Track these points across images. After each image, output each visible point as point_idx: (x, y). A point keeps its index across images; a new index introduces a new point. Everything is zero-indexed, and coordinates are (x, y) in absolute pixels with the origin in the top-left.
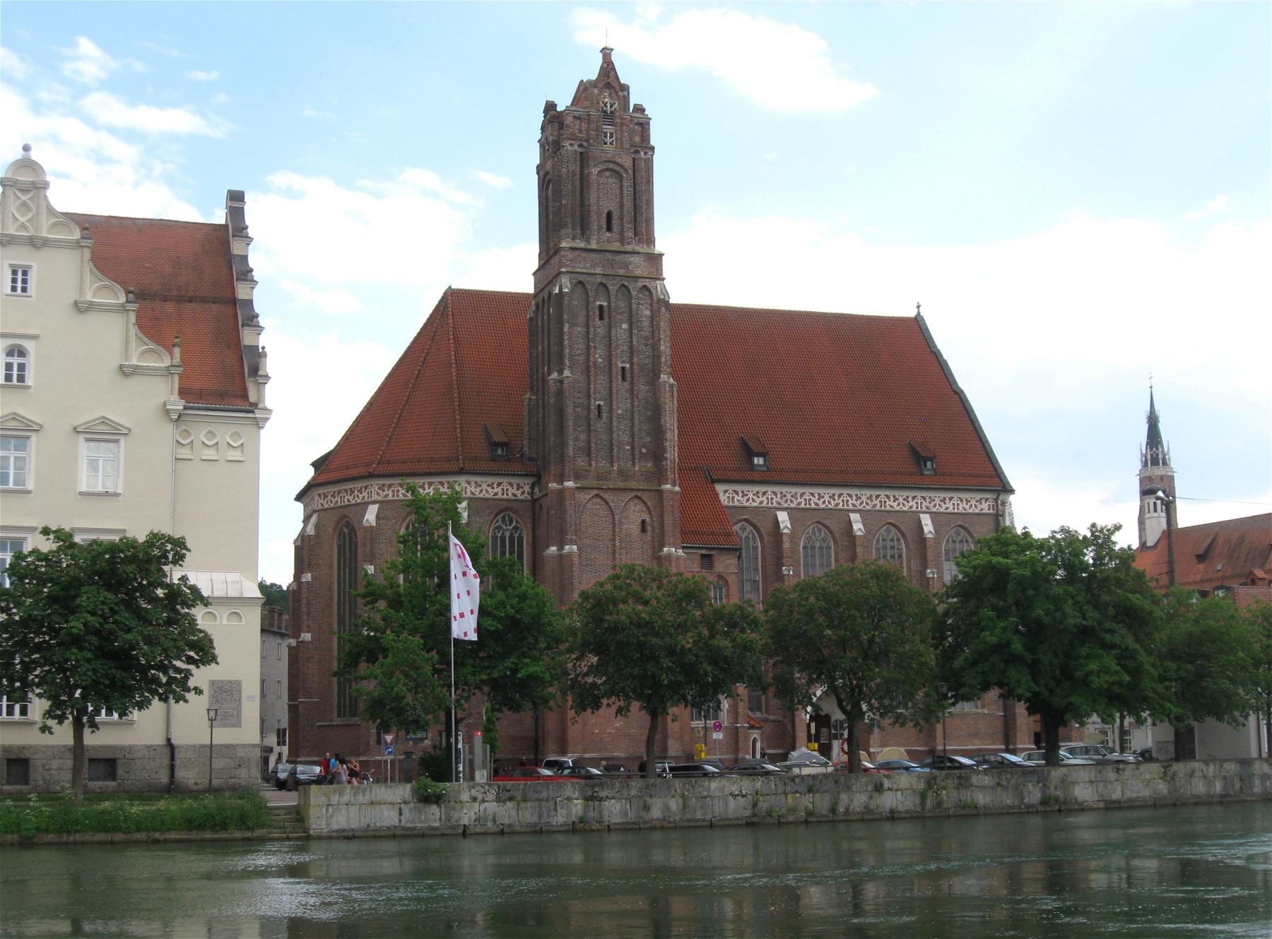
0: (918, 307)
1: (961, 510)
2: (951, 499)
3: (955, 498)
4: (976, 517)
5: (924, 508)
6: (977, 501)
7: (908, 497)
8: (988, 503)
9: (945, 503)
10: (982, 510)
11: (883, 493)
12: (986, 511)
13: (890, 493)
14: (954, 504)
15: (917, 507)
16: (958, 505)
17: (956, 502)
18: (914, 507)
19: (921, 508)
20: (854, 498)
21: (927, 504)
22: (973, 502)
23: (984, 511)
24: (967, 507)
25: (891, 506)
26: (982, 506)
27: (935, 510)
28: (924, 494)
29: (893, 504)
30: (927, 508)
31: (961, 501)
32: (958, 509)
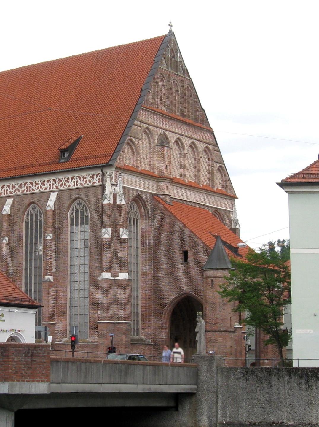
0: (170, 26)
1: (79, 186)
2: (72, 178)
3: (76, 177)
4: (90, 189)
5: (54, 187)
6: (90, 177)
7: (44, 181)
8: (98, 177)
9: (68, 182)
10: (94, 183)
11: (28, 181)
12: (97, 184)
13: (33, 180)
14: (74, 182)
15: (50, 188)
16: (77, 182)
17: (76, 181)
18: (48, 188)
19: (53, 188)
20: (11, 187)
21: (56, 185)
22: (88, 178)
23: (95, 184)
24: (83, 183)
25: (33, 190)
26: (94, 180)
27: (61, 188)
28: (55, 177)
29: (34, 188)
30: (57, 187)
31: (80, 178)
32: (77, 185)
